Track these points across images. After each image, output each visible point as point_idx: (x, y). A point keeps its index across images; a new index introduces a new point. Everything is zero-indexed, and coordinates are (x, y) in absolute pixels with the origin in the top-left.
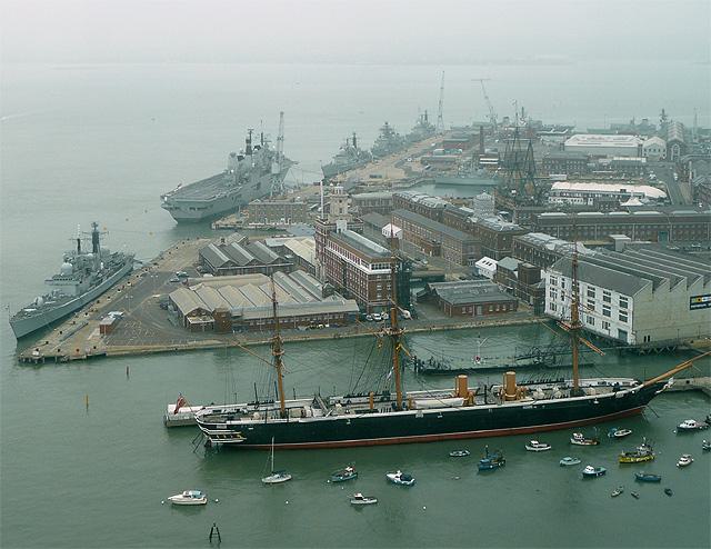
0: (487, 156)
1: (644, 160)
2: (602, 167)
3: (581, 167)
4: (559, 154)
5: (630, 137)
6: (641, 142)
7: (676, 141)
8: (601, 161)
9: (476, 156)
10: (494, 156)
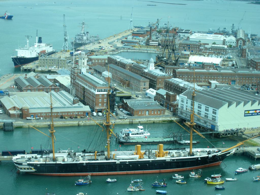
0: (153, 41)
1: (226, 47)
2: (206, 49)
3: (197, 48)
4: (188, 42)
5: (220, 36)
6: (225, 38)
7: (241, 39)
8: (206, 46)
9: (148, 41)
10: (156, 41)
